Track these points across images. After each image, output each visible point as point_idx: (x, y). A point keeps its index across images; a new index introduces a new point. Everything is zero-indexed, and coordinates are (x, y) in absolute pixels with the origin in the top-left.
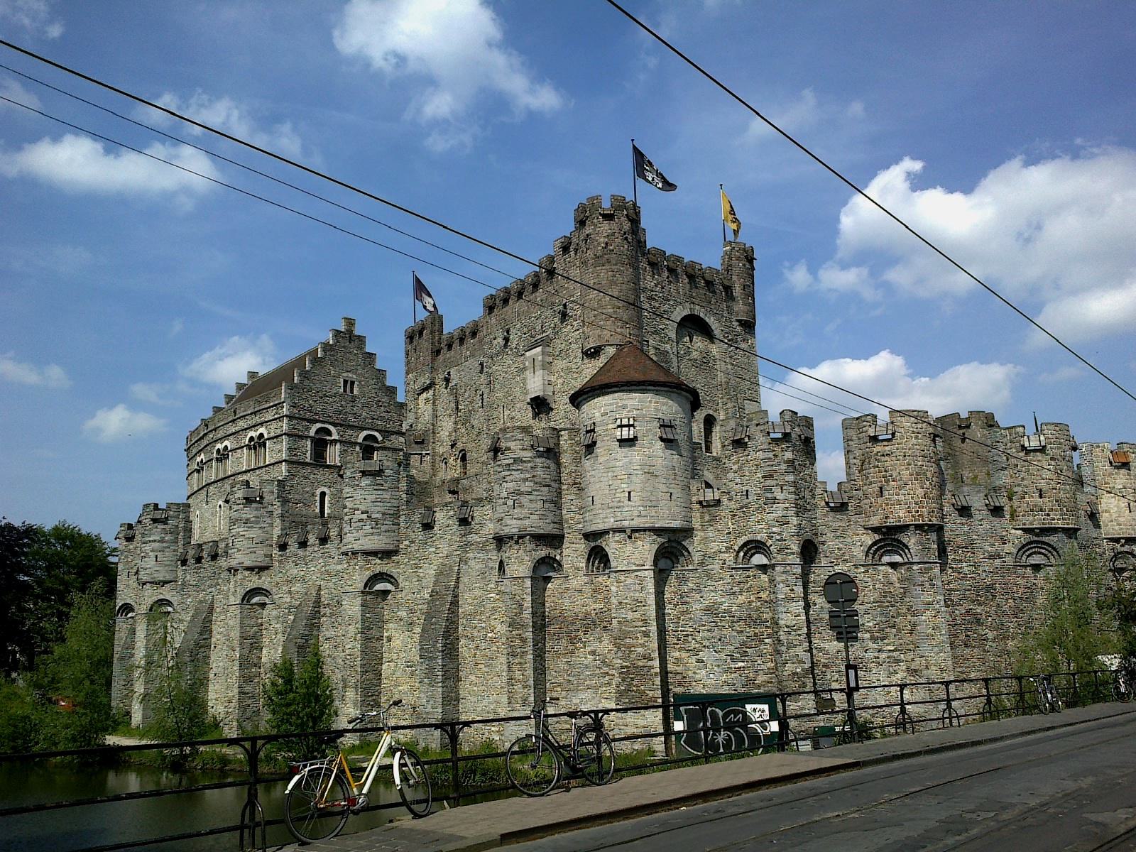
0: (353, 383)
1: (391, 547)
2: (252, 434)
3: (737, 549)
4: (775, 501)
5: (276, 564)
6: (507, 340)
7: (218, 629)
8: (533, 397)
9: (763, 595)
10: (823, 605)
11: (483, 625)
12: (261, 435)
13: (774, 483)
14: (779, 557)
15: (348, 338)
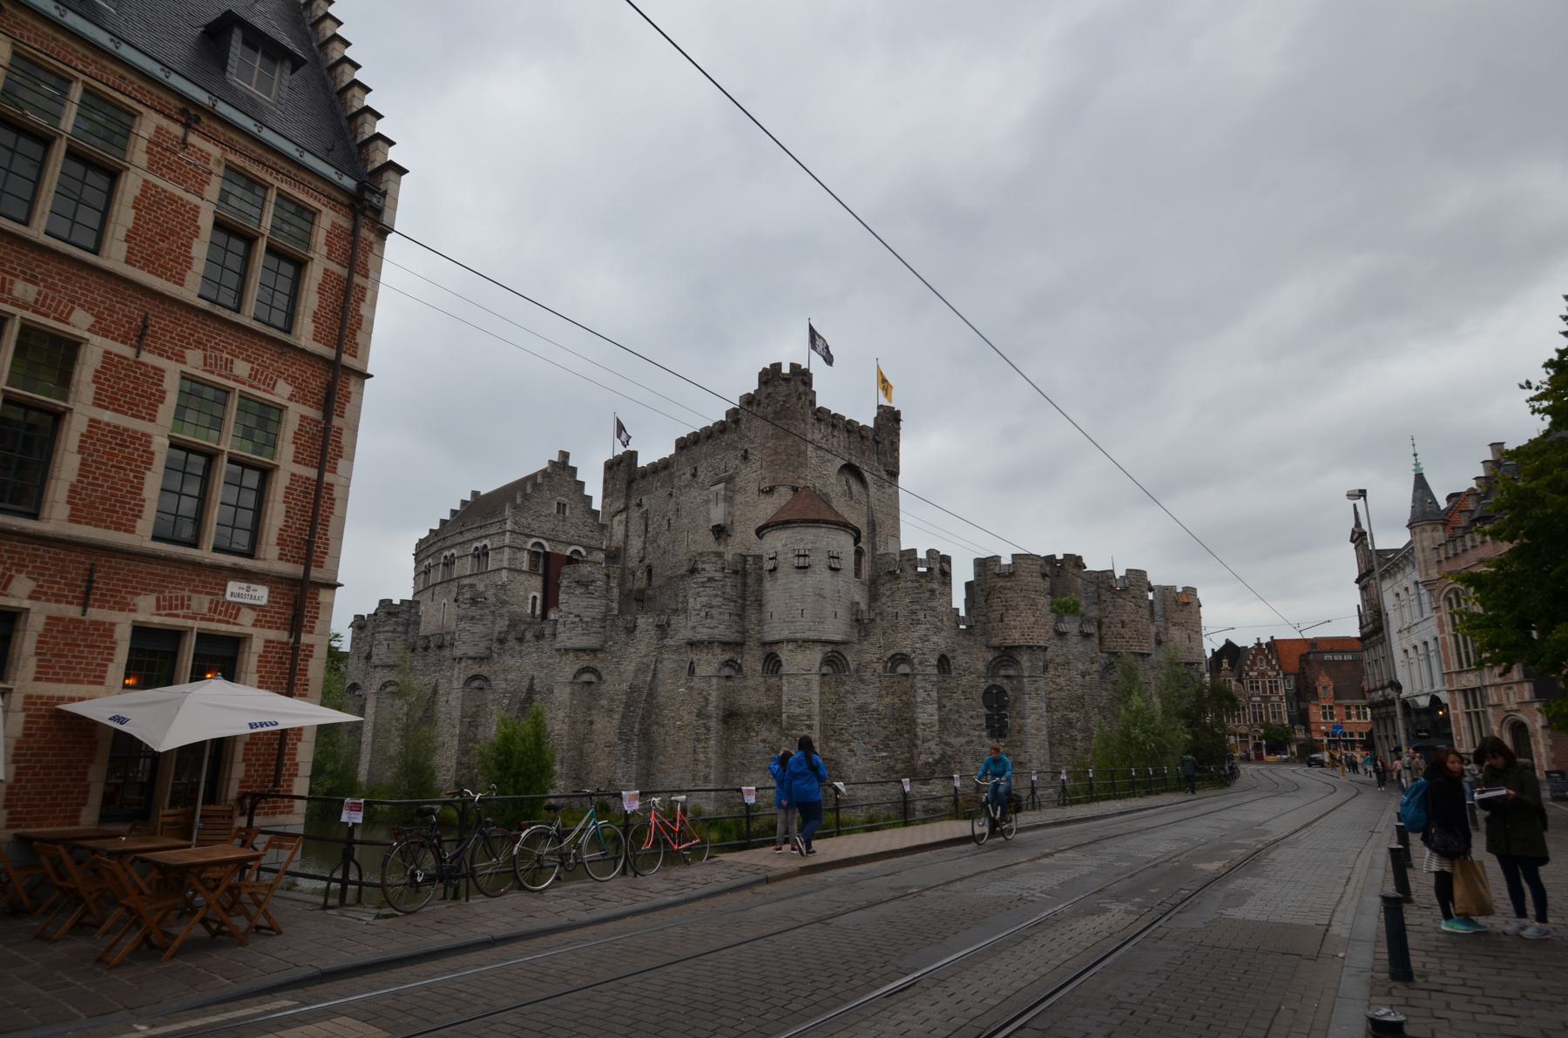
0: (565, 505)
1: (598, 646)
2: (477, 544)
3: (886, 659)
4: (918, 622)
5: (495, 656)
6: (694, 475)
7: (441, 708)
8: (715, 524)
9: (904, 698)
12: (485, 546)
13: (918, 607)
14: (920, 668)
15: (562, 469)
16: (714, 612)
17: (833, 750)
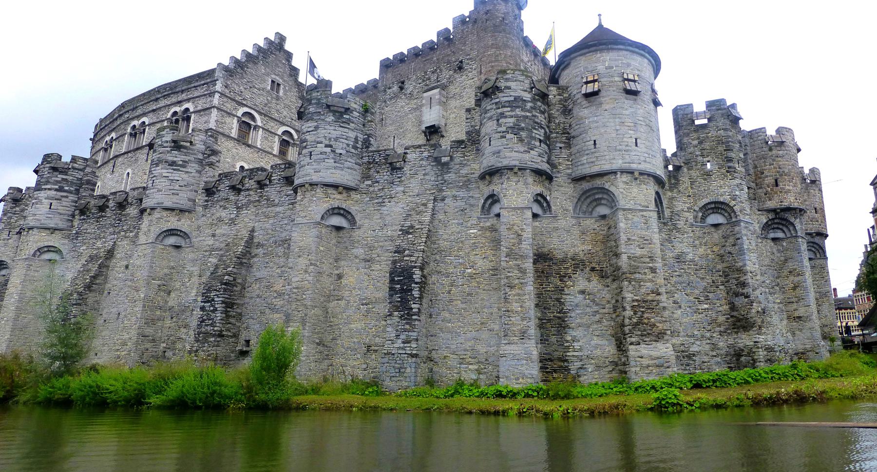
3: (697, 209)
11: (460, 261)
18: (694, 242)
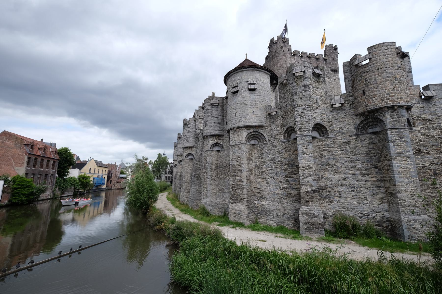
1: (192, 146)
3: (284, 132)
4: (298, 106)
10: (330, 156)
16: (208, 123)
17: (259, 183)
18: (282, 151)
